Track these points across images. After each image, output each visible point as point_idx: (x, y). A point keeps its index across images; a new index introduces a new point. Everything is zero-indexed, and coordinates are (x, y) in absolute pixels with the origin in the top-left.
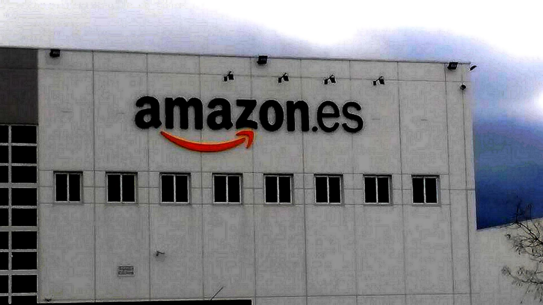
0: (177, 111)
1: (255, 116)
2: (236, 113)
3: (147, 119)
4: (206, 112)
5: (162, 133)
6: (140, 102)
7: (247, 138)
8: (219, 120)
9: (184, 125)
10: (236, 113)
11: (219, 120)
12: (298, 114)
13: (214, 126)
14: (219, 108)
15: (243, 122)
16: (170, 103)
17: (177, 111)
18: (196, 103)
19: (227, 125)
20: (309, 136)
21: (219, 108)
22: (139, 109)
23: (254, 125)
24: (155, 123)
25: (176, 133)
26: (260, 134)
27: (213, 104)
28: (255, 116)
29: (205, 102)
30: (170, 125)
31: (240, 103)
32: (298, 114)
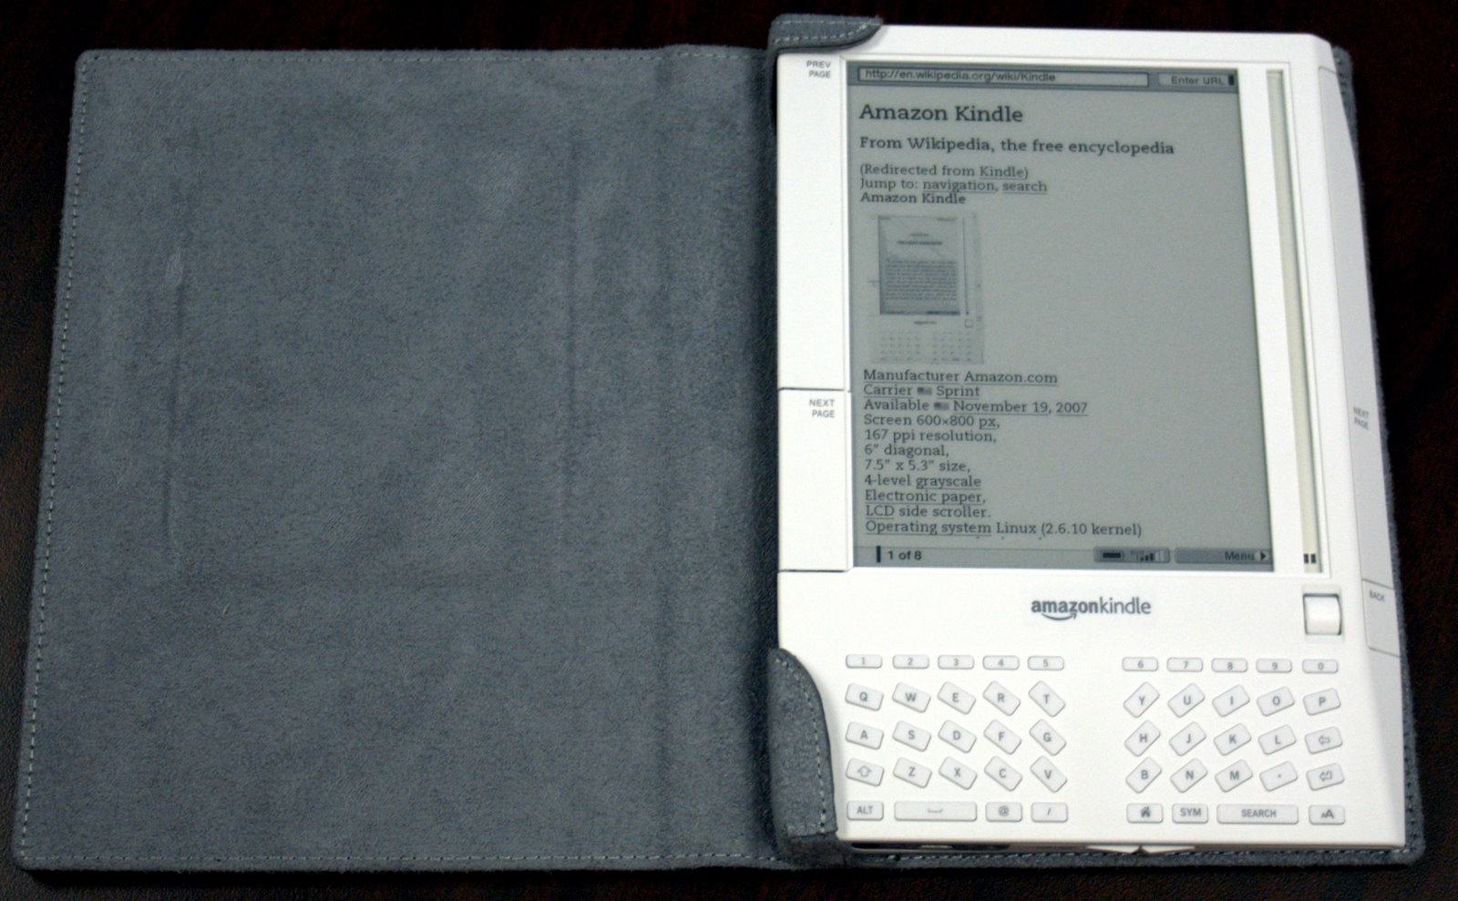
0: (1047, 606)
1: (1077, 608)
2: (1069, 606)
3: (1036, 608)
4: (1058, 606)
6: (1034, 603)
10: (1069, 606)
12: (1093, 607)
13: (1061, 611)
15: (1072, 609)
16: (1045, 603)
17: (1047, 606)
18: (1054, 603)
19: (1066, 610)
22: (1031, 606)
23: (1076, 611)
24: (1039, 610)
25: (1047, 613)
26: (1079, 614)
30: (1044, 611)
31: (1071, 603)
32: (1093, 607)
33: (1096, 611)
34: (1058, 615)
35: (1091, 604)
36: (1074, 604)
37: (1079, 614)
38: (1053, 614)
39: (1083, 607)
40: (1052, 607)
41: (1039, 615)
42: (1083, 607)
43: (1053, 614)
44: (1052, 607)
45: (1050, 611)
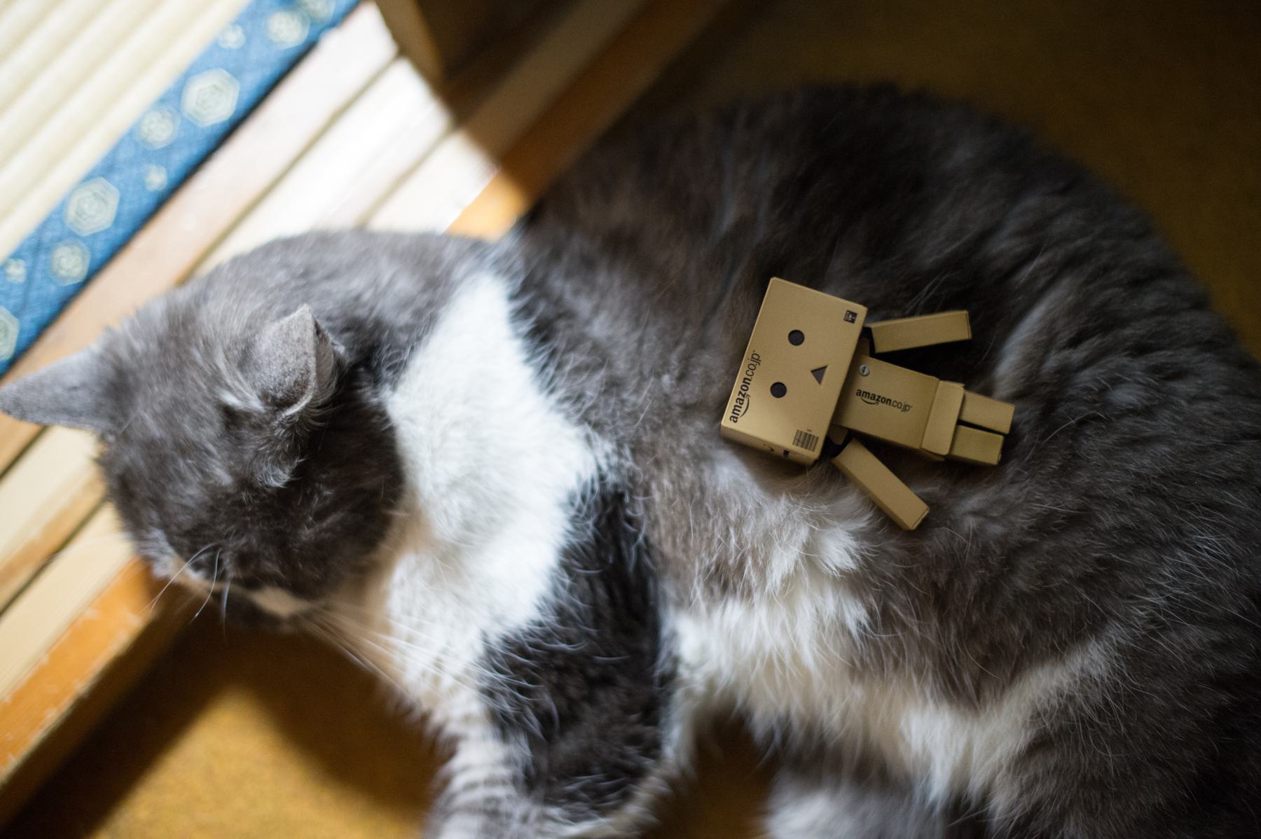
0: (735, 412)
4: (738, 404)
9: (739, 411)
10: (741, 397)
12: (746, 381)
13: (742, 404)
15: (744, 396)
17: (735, 412)
19: (743, 400)
20: (753, 380)
24: (737, 418)
25: (741, 414)
27: (737, 402)
28: (743, 392)
29: (736, 404)
30: (738, 415)
32: (746, 381)
35: (744, 382)
39: (743, 388)
40: (737, 408)
44: (737, 408)
45: (739, 411)
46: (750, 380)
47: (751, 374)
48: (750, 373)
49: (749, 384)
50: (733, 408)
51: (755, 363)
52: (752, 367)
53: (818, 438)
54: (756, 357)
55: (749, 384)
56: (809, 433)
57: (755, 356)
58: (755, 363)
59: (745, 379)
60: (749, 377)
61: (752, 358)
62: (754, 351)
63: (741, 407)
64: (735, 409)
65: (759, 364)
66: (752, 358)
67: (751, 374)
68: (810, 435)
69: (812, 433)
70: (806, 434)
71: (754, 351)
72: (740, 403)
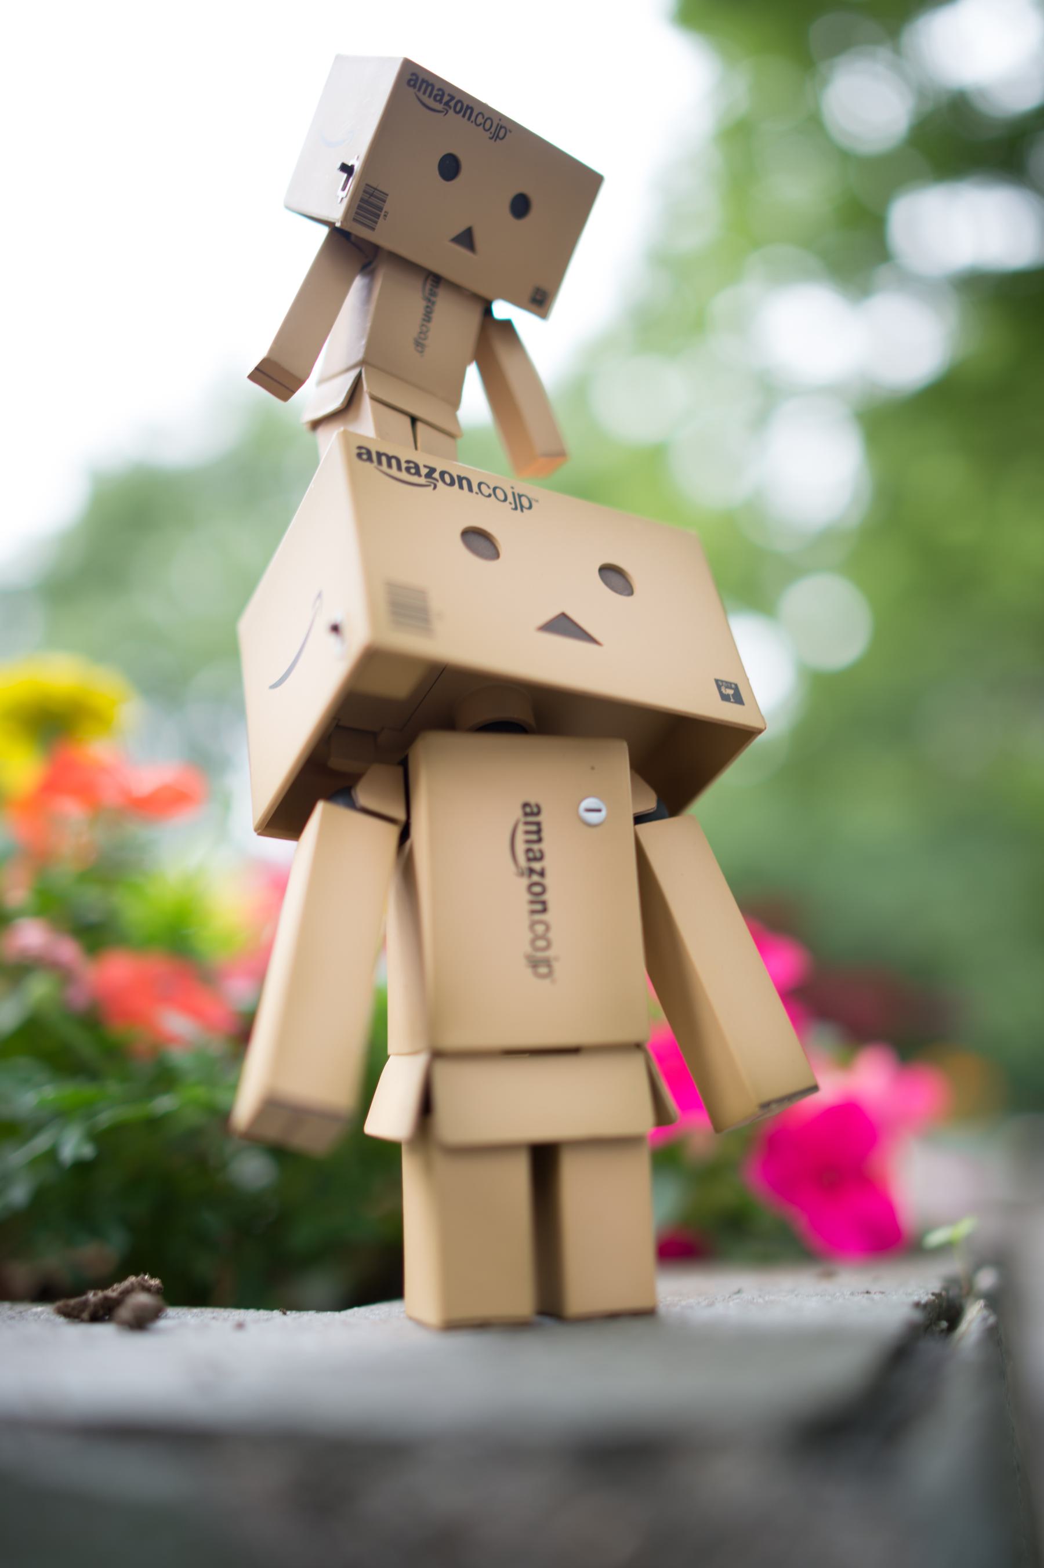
0: (424, 85)
1: (452, 104)
2: (446, 98)
3: (412, 83)
4: (435, 92)
5: (415, 93)
7: (445, 112)
8: (438, 98)
9: (424, 93)
10: (446, 98)
11: (438, 98)
14: (440, 93)
15: (447, 104)
16: (423, 81)
17: (424, 85)
18: (433, 86)
19: (440, 101)
21: (440, 93)
23: (450, 107)
24: (414, 86)
25: (420, 94)
26: (451, 112)
27: (439, 90)
28: (452, 104)
29: (436, 88)
30: (419, 90)
31: (449, 95)
33: (469, 119)
34: (431, 102)
35: (468, 107)
36: (452, 98)
37: (451, 112)
38: (425, 99)
40: (430, 88)
41: (411, 90)
42: (458, 108)
43: (425, 99)
44: (430, 88)
45: (424, 93)
46: (469, 119)
47: (478, 122)
48: (480, 120)
49: (464, 116)
50: (430, 82)
51: (493, 130)
52: (489, 123)
53: (373, 229)
54: (501, 135)
55: (464, 116)
56: (383, 214)
57: (503, 131)
58: (493, 130)
59: (472, 110)
60: (473, 118)
61: (501, 127)
62: (510, 132)
63: (430, 96)
64: (428, 84)
65: (491, 138)
66: (501, 127)
67: (478, 122)
68: (378, 216)
69: (381, 220)
70: (381, 209)
71: (510, 132)
72: (436, 95)
